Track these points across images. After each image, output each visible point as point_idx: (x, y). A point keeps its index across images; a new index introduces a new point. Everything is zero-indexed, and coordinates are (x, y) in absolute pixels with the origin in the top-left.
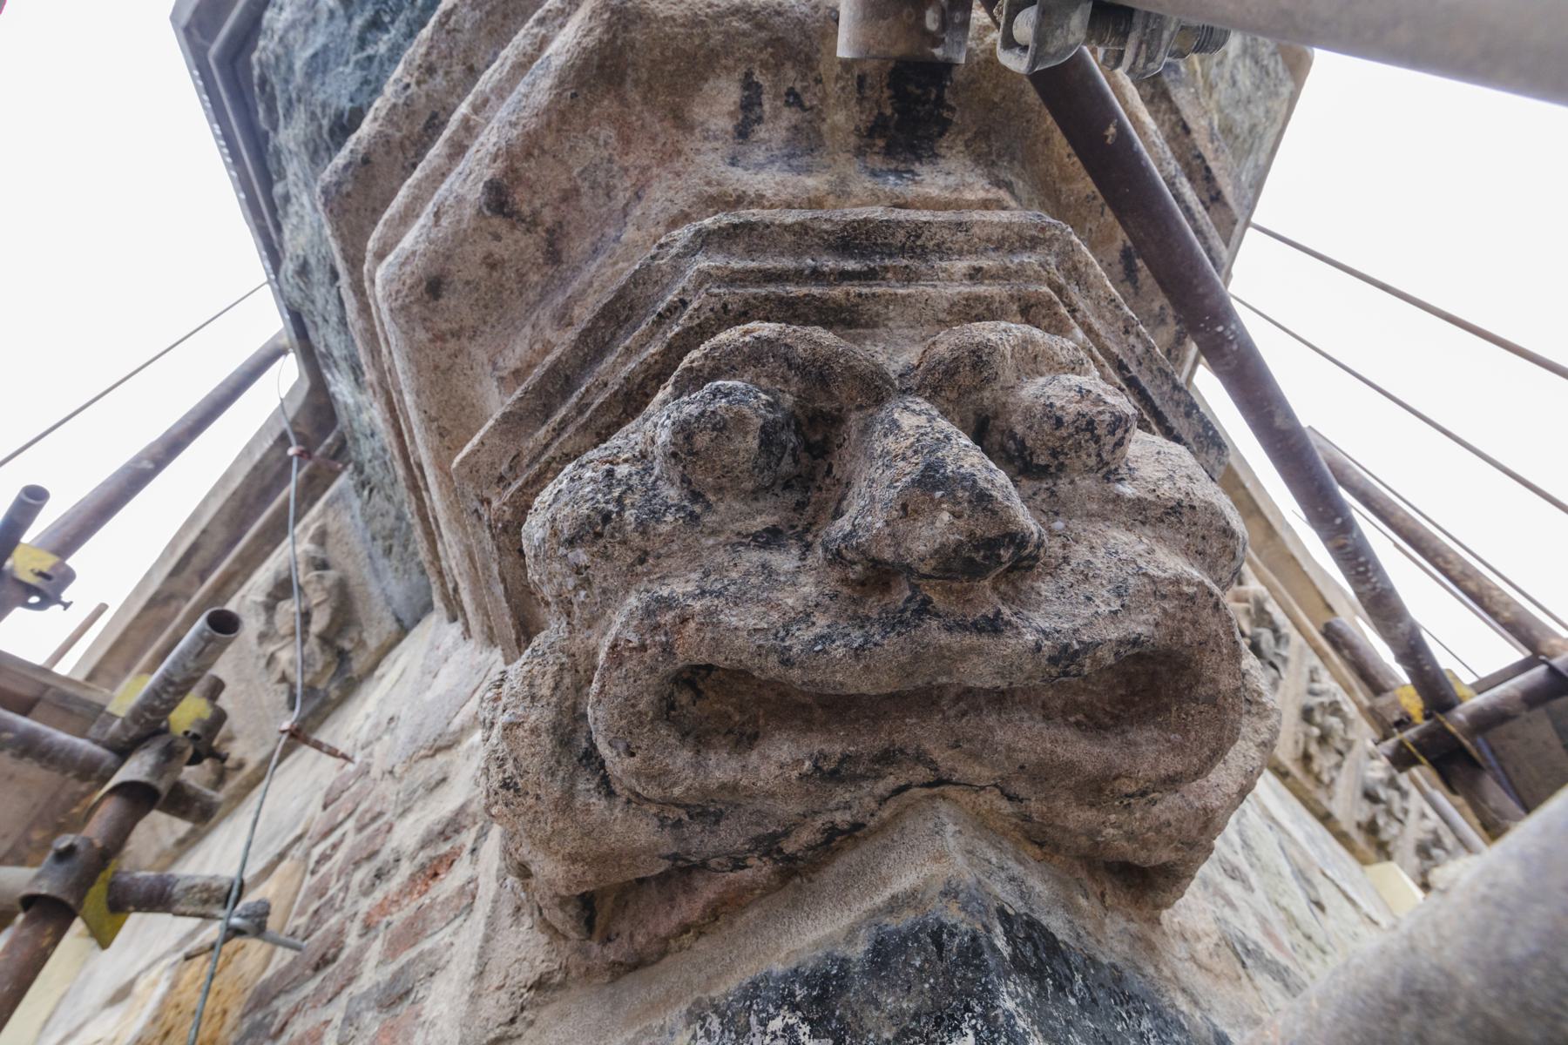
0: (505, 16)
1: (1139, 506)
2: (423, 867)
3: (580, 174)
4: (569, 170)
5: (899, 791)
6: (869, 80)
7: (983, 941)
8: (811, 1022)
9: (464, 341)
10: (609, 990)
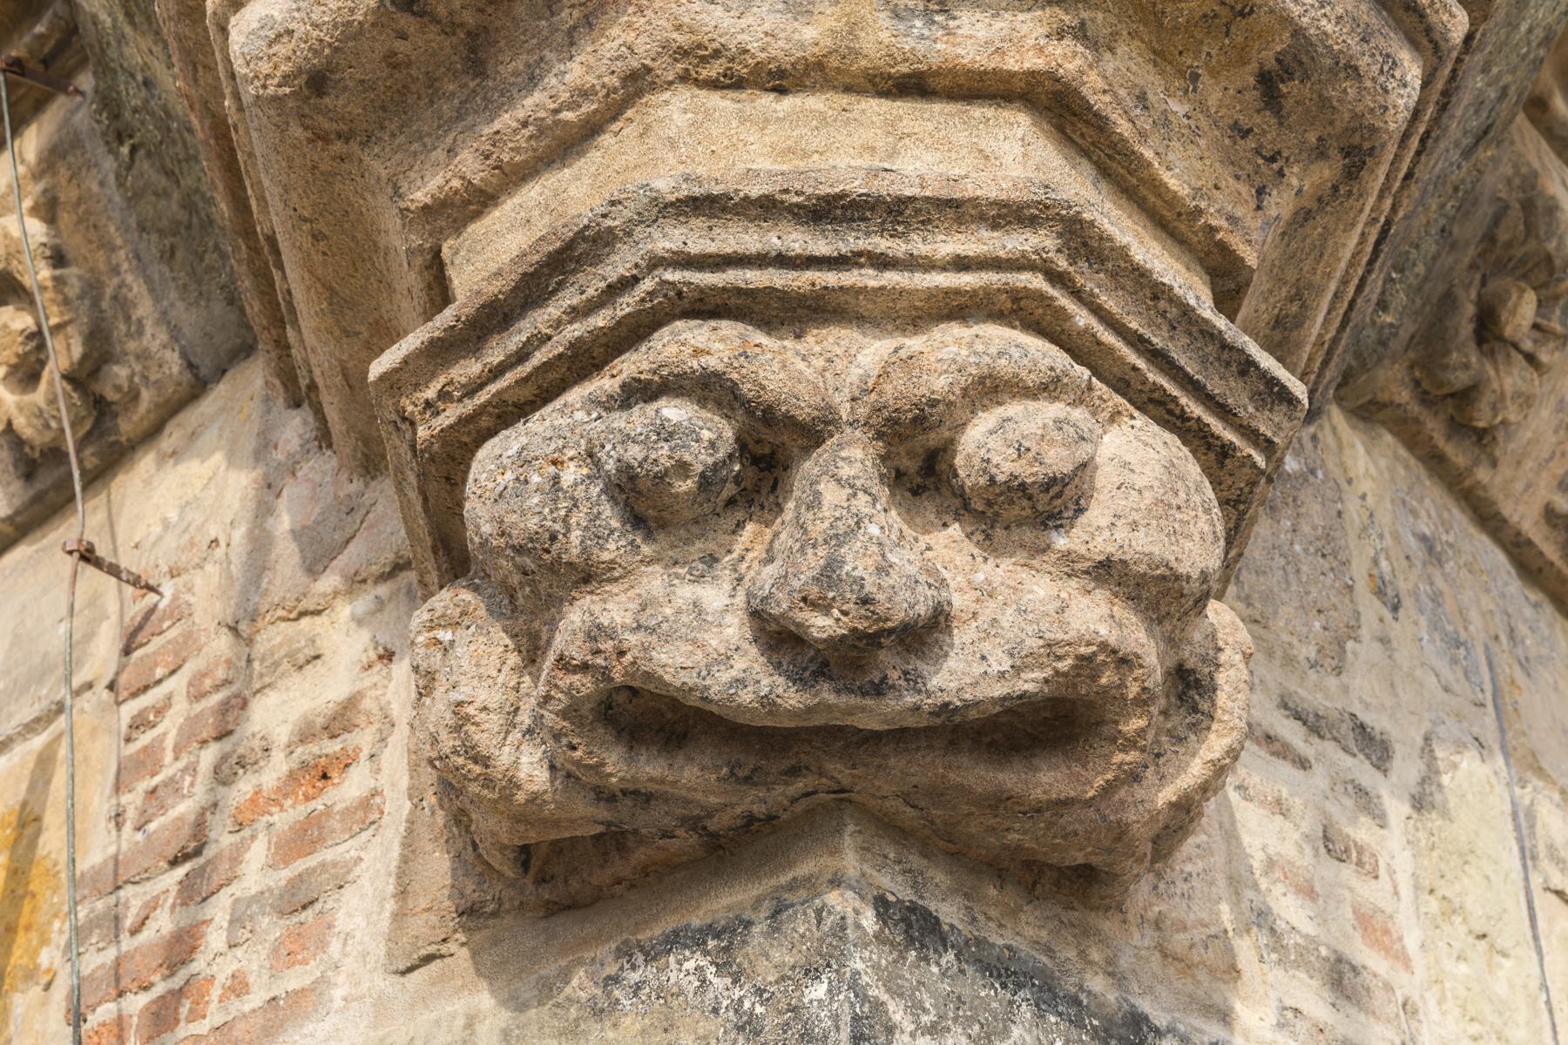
1: (1067, 557)
2: (304, 766)
5: (808, 794)
7: (849, 921)
8: (717, 965)
9: (354, 147)
10: (542, 924)
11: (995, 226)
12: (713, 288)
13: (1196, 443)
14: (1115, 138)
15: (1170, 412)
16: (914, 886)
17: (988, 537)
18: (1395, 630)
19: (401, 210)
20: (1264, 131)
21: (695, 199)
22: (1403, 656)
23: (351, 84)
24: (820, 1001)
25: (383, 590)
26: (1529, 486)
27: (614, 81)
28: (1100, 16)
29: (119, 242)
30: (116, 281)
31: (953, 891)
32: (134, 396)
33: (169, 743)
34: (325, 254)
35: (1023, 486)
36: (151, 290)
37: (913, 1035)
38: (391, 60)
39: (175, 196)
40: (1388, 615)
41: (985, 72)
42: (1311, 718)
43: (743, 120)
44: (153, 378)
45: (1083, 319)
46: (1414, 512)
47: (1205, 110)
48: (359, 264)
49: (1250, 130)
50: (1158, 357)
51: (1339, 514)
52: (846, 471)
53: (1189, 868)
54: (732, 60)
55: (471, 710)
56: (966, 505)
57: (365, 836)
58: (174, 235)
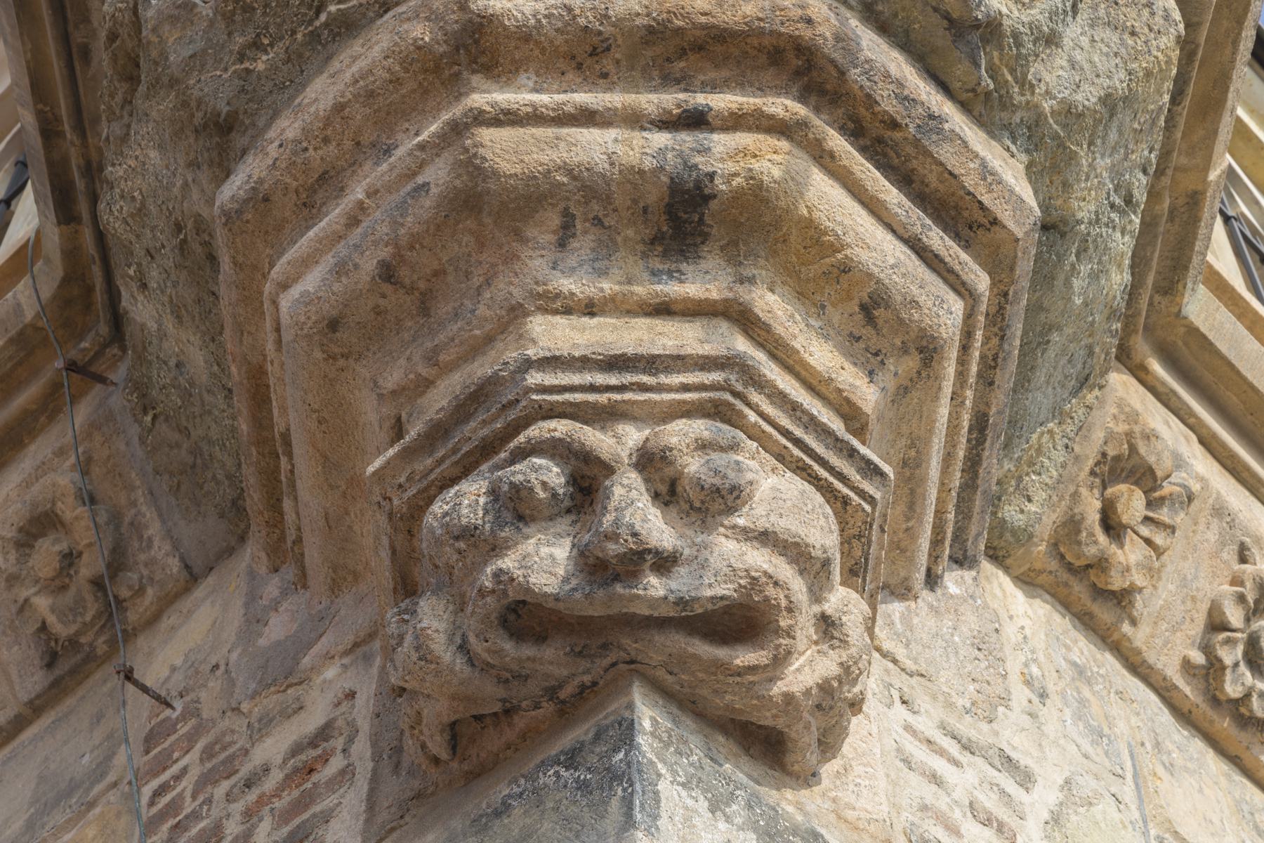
0: (388, 114)
1: (745, 530)
2: (296, 770)
4: (440, 260)
5: (614, 665)
9: (351, 361)
11: (702, 369)
12: (558, 402)
15: (809, 475)
16: (674, 720)
18: (1043, 712)
19: (378, 395)
22: (1051, 728)
23: (352, 325)
24: (621, 761)
25: (346, 661)
27: (504, 313)
29: (138, 483)
30: (133, 511)
32: (141, 591)
33: (188, 794)
36: (160, 515)
37: (672, 783)
38: (378, 311)
40: (1036, 700)
41: (701, 301)
42: (964, 740)
44: (157, 578)
45: (752, 417)
46: (1068, 648)
49: (860, 338)
50: (798, 442)
51: (997, 631)
52: (625, 482)
53: (858, 780)
55: (429, 632)
56: (692, 507)
57: (342, 790)
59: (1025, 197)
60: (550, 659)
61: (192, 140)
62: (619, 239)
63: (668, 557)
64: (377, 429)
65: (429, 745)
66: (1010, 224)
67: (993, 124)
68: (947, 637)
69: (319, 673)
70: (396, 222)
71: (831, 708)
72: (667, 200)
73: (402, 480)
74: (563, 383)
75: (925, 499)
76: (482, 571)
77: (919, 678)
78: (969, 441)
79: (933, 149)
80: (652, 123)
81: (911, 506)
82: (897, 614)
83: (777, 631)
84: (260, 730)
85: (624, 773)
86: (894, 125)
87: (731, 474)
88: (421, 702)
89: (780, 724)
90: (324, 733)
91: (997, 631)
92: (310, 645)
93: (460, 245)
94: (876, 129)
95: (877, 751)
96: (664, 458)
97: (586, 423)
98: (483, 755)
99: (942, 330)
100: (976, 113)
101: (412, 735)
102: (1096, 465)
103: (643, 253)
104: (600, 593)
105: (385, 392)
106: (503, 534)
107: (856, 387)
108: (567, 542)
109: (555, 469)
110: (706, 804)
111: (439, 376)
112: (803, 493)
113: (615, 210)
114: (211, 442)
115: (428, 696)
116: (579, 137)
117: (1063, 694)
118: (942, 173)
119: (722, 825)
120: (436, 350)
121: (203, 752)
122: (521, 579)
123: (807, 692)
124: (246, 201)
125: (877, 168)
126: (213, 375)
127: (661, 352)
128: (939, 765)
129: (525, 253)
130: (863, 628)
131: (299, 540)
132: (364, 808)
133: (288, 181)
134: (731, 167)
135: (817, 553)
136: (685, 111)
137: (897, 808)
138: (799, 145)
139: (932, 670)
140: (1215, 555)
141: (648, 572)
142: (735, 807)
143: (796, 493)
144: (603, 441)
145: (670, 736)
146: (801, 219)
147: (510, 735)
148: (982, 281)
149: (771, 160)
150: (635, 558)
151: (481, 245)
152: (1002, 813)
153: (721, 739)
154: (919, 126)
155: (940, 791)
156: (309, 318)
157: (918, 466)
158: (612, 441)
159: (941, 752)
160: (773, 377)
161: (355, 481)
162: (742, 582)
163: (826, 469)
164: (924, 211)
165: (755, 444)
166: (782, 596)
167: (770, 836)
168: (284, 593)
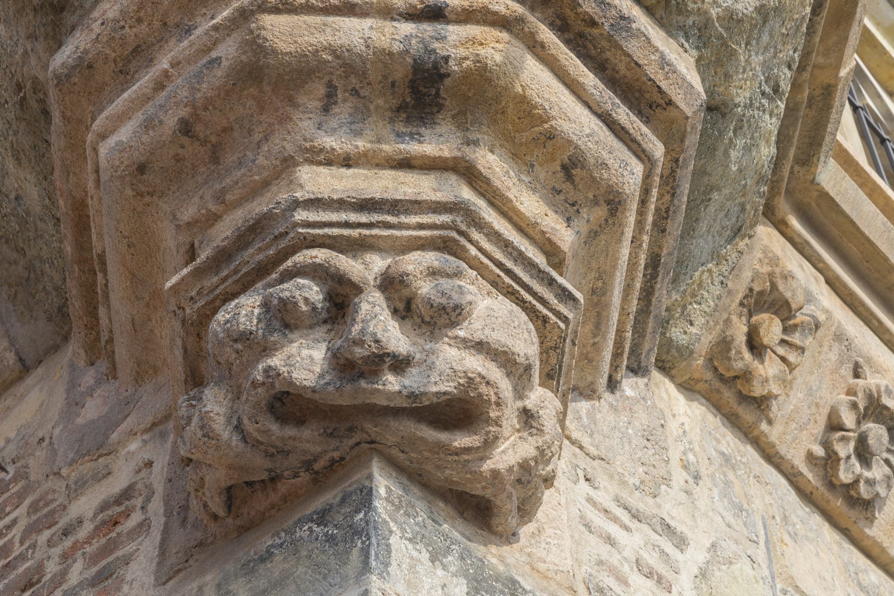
1: (464, 340)
2: (104, 523)
3: (234, 120)
4: (228, 119)
5: (358, 444)
6: (397, 84)
9: (155, 198)
11: (434, 212)
12: (319, 235)
13: (532, 315)
14: (495, 188)
15: (517, 298)
16: (404, 489)
17: (432, 333)
18: (697, 490)
19: (176, 225)
20: (568, 192)
21: (312, 200)
22: (702, 504)
23: (157, 169)
24: (361, 519)
25: (146, 437)
26: (795, 439)
27: (278, 163)
28: (486, 137)
31: (423, 498)
33: (17, 540)
34: (133, 254)
35: (444, 308)
38: (178, 159)
39: (22, 263)
40: (691, 481)
41: (435, 158)
42: (634, 511)
43: (333, 177)
45: (473, 251)
47: (539, 181)
48: (149, 260)
49: (561, 191)
50: (508, 272)
52: (371, 299)
53: (549, 540)
54: (327, 152)
55: (212, 415)
56: (423, 321)
57: (140, 539)
58: (18, 285)
59: (694, 84)
60: (308, 438)
61: (31, 17)
62: (372, 107)
63: (403, 360)
64: (175, 253)
65: (210, 504)
66: (682, 105)
67: (671, 25)
68: (623, 429)
69: (124, 446)
70: (193, 88)
71: (529, 482)
72: (410, 77)
73: (193, 293)
74: (324, 220)
75: (608, 321)
76: (255, 367)
77: (600, 461)
78: (644, 275)
79: (623, 43)
80: (400, 15)
81: (598, 325)
82: (584, 411)
83: (488, 421)
84: (76, 490)
85: (363, 529)
86: (593, 23)
87: (455, 296)
88: (204, 470)
89: (488, 493)
90: (127, 494)
91: (662, 426)
92: (117, 425)
93: (245, 107)
94: (578, 26)
95: (565, 517)
96: (402, 282)
97: (341, 252)
98: (252, 513)
99: (626, 187)
100: (658, 16)
101: (197, 497)
102: (744, 298)
103: (391, 118)
104: (348, 387)
105: (182, 223)
106: (272, 339)
107: (557, 230)
108: (323, 346)
109: (316, 288)
110: (428, 555)
111: (225, 212)
112: (511, 312)
113: (369, 84)
114: (42, 261)
115: (210, 466)
116: (342, 24)
117: (712, 477)
118: (629, 62)
119: (440, 572)
120: (224, 191)
121: (30, 507)
122: (286, 374)
123: (510, 469)
124: (74, 67)
125: (578, 57)
126: (45, 207)
127: (402, 197)
128: (613, 529)
129: (296, 115)
130: (555, 420)
131: (111, 340)
132: (157, 553)
133: (108, 52)
134: (462, 52)
135: (521, 360)
136: (427, 6)
137: (578, 562)
138: (517, 36)
139: (610, 455)
140: (835, 371)
141: (386, 371)
142: (450, 558)
143: (506, 312)
144: (354, 267)
145: (401, 501)
146: (517, 95)
147: (274, 498)
148: (658, 150)
149: (494, 48)
150: (377, 360)
151: (262, 109)
152: (661, 568)
153: (441, 504)
154: (612, 25)
155: (613, 550)
156: (122, 162)
157: (604, 294)
158: (361, 267)
159: (615, 520)
160: (490, 220)
161: (156, 294)
162: (461, 381)
163: (530, 294)
164: (615, 93)
165: (475, 273)
166: (492, 393)
167: (477, 581)
168: (98, 382)
